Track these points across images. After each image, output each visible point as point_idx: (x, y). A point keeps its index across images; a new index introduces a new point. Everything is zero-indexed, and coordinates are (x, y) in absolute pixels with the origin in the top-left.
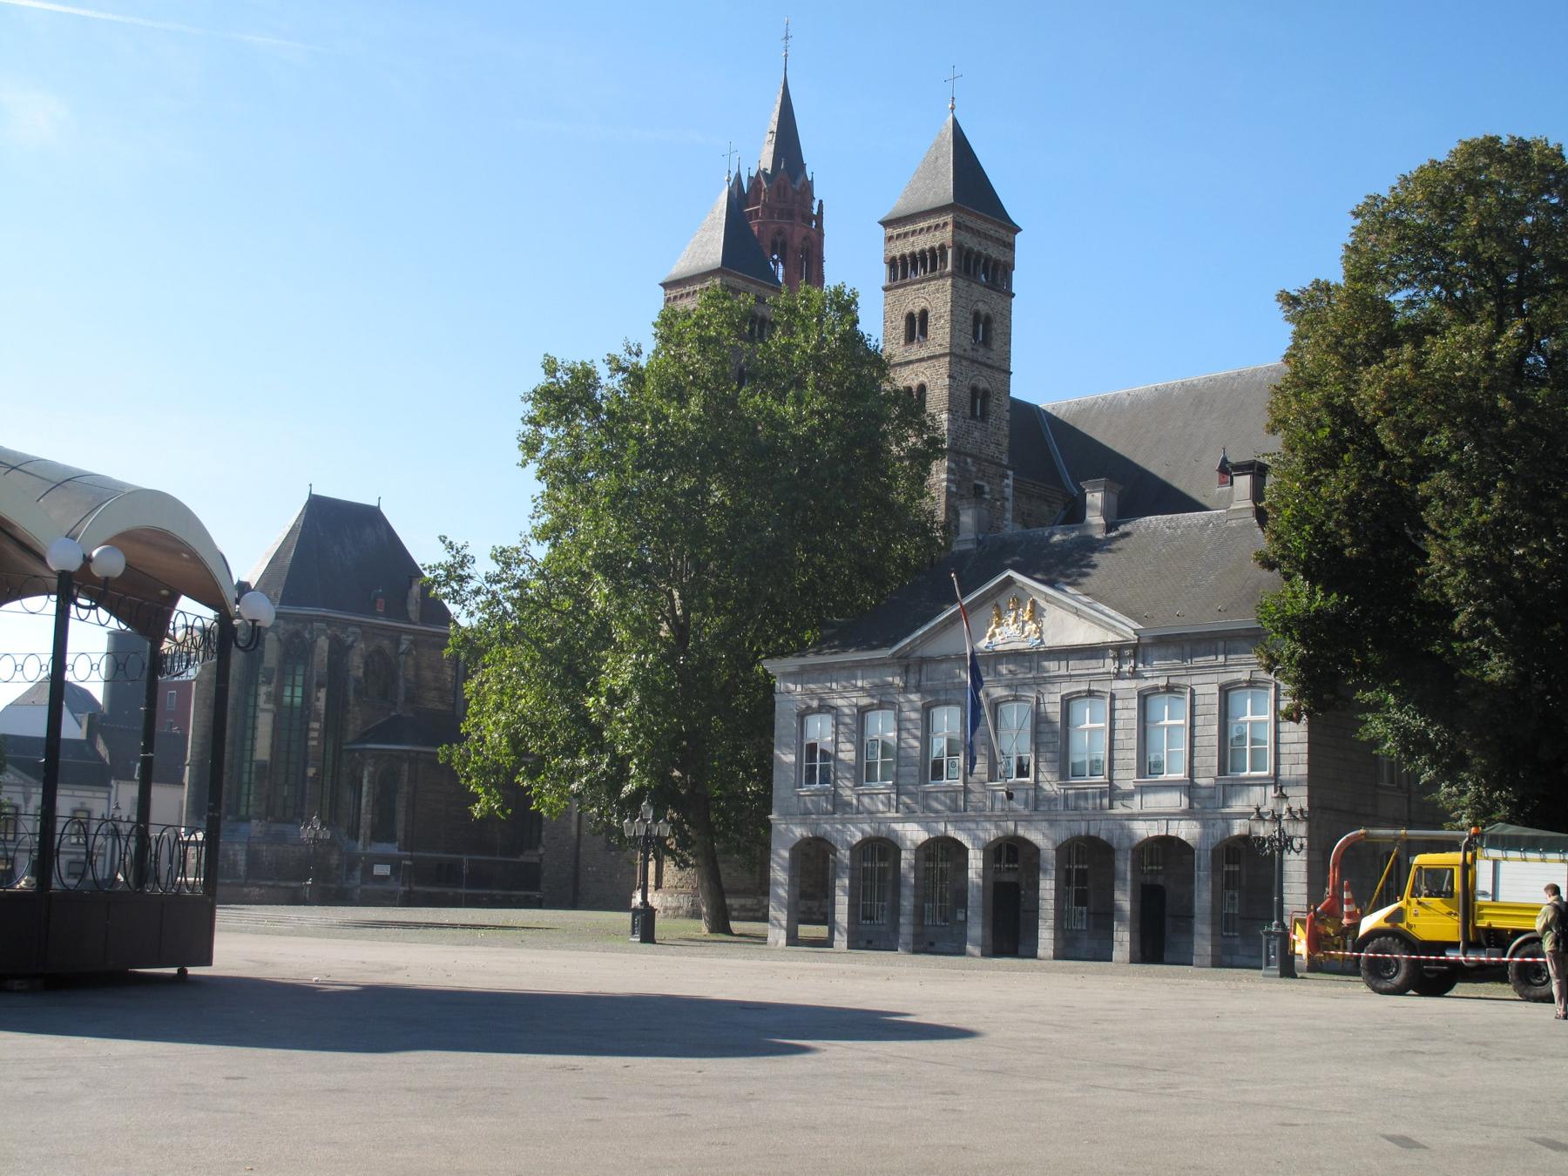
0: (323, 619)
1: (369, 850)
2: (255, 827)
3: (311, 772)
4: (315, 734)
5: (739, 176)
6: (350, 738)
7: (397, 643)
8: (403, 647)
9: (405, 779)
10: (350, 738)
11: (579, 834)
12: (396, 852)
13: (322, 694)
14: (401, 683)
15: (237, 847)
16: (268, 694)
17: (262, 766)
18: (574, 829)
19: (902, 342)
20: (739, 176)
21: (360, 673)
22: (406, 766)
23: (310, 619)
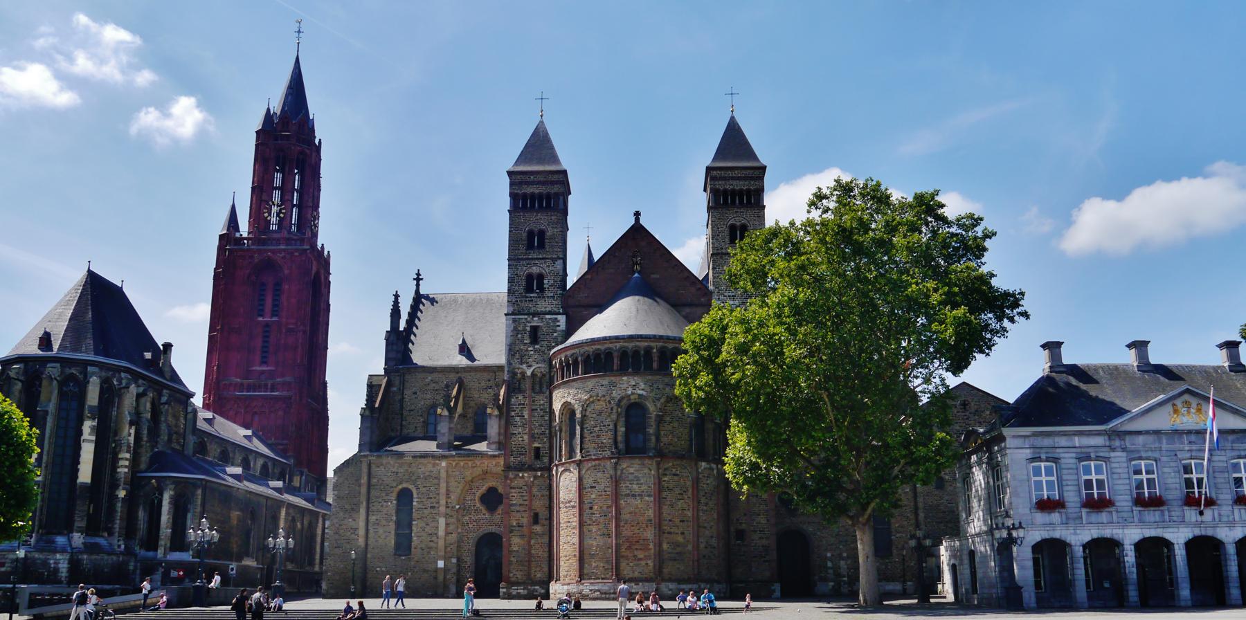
0: (128, 370)
1: (169, 557)
2: (78, 539)
3: (122, 494)
4: (127, 463)
5: (268, 110)
6: (143, 466)
7: (160, 395)
8: (164, 399)
9: (199, 502)
10: (143, 466)
11: (367, 545)
12: (191, 559)
13: (132, 431)
14: (163, 427)
15: (58, 556)
16: (92, 428)
17: (84, 485)
18: (361, 541)
19: (727, 240)
20: (268, 110)
21: (149, 416)
22: (199, 492)
23: (119, 369)
